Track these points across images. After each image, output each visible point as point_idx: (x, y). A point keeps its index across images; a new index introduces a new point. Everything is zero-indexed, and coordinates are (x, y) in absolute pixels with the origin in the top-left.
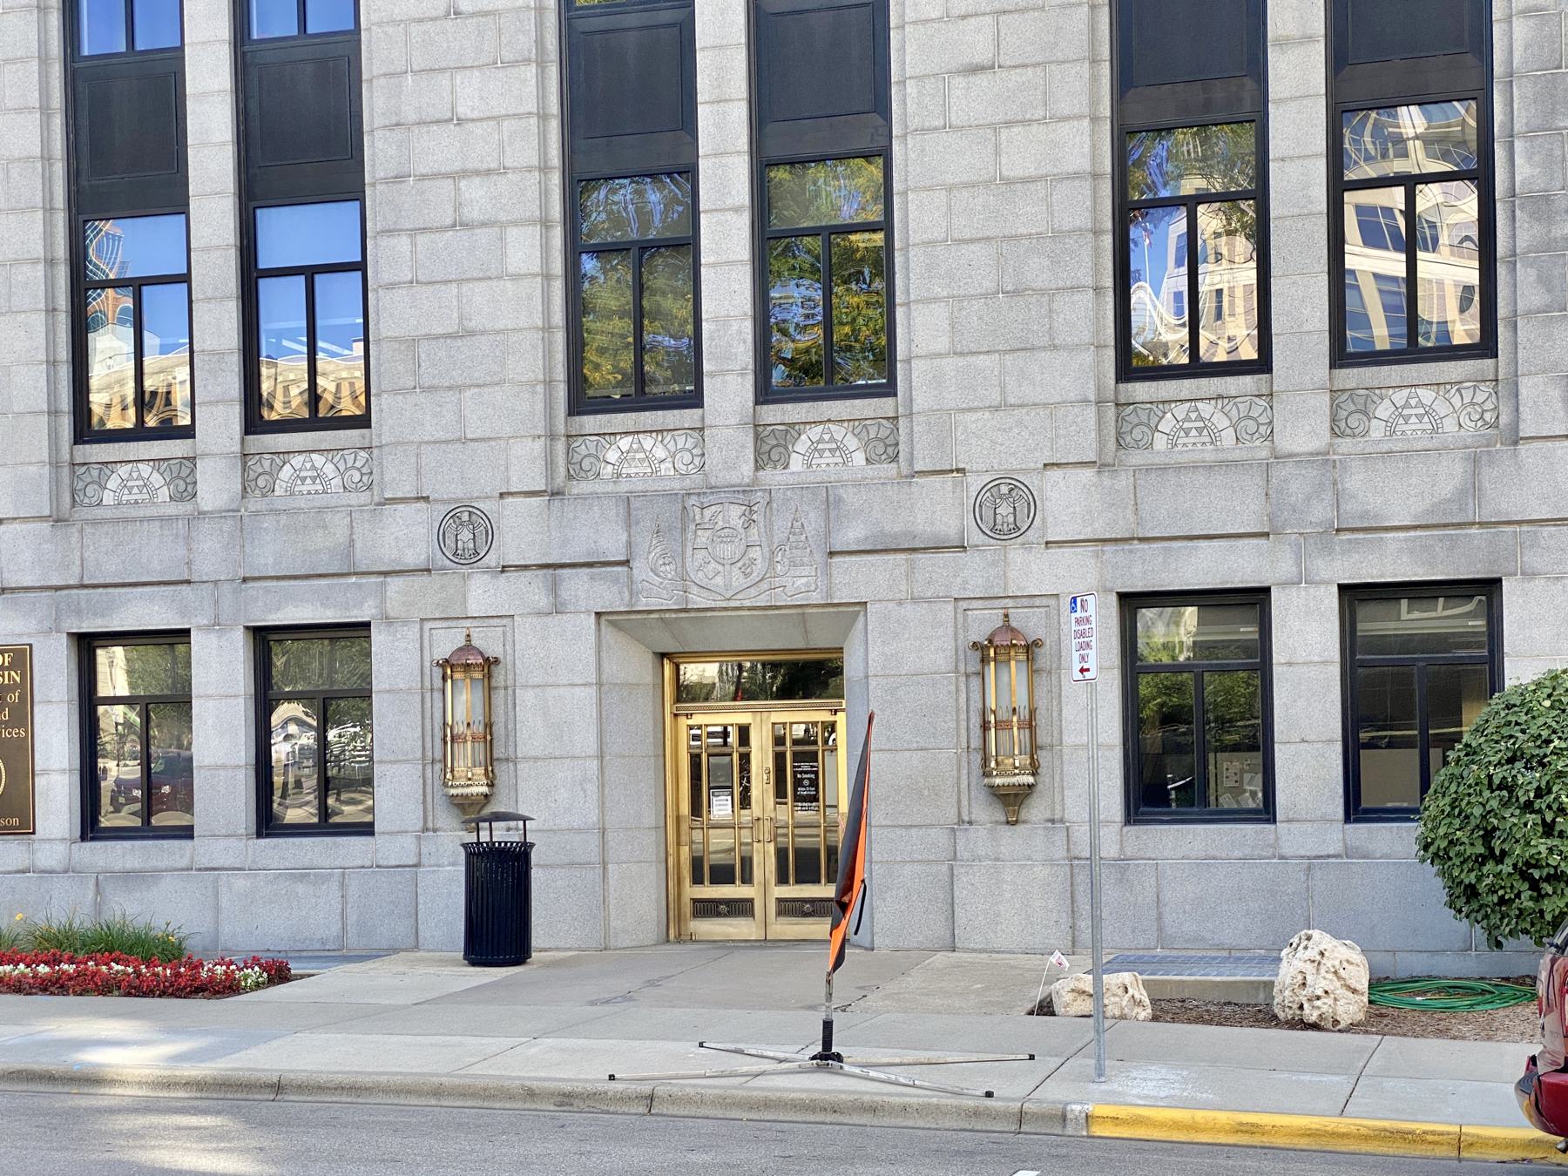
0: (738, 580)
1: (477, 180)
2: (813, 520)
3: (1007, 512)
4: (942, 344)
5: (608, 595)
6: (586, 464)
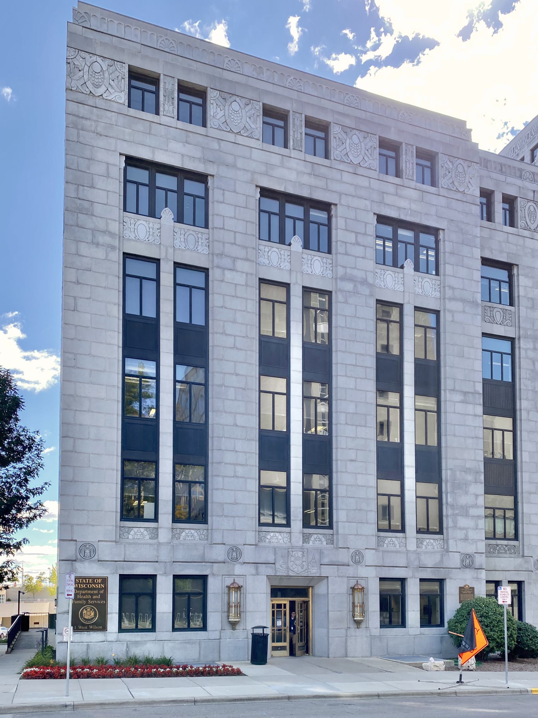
0: (300, 570)
1: (240, 467)
2: (317, 557)
4: (345, 520)
5: (271, 572)
6: (262, 538)
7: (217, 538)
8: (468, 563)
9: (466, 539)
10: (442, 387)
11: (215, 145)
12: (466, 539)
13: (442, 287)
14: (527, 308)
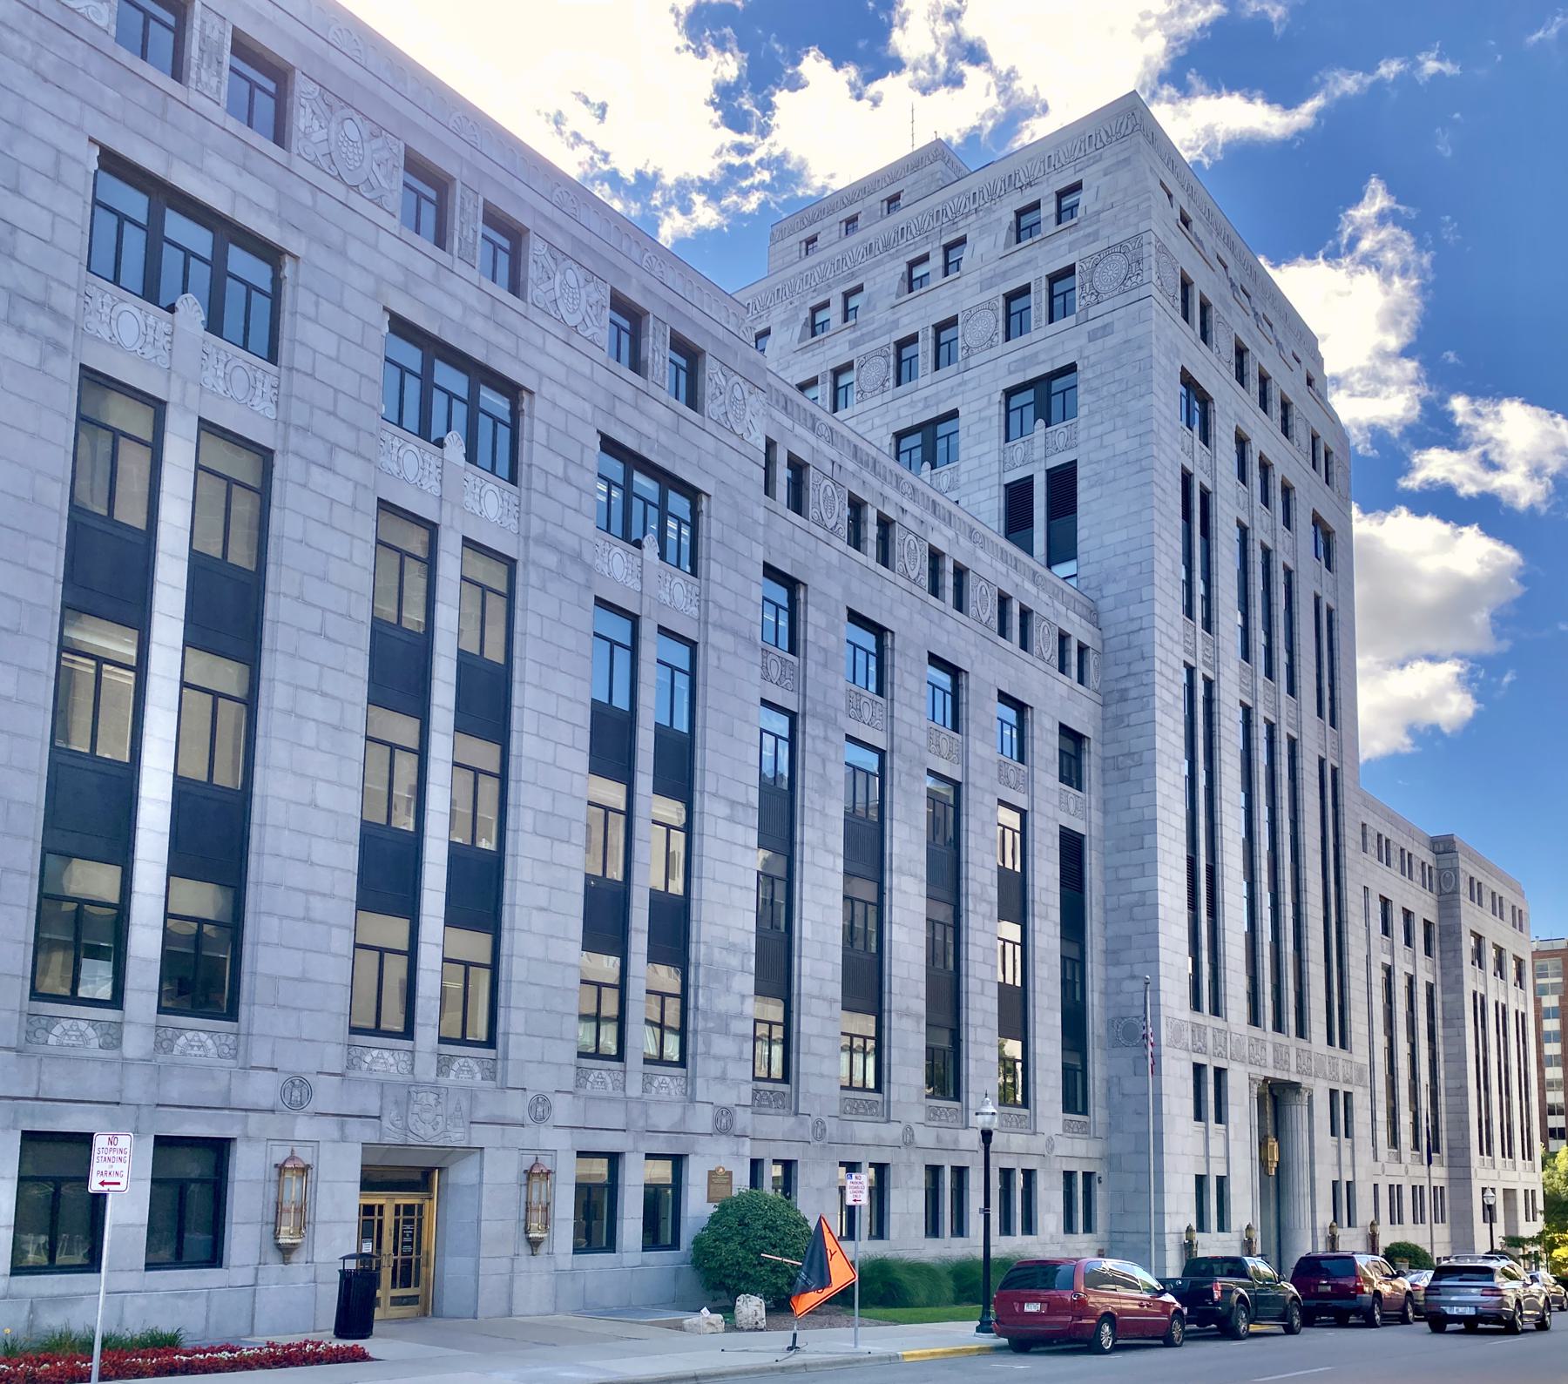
0: (431, 1132)
2: (465, 1105)
3: (540, 1110)
5: (370, 1135)
7: (261, 1055)
8: (724, 1126)
9: (723, 1078)
10: (697, 786)
11: (305, 195)
12: (723, 1078)
13: (704, 601)
14: (817, 663)
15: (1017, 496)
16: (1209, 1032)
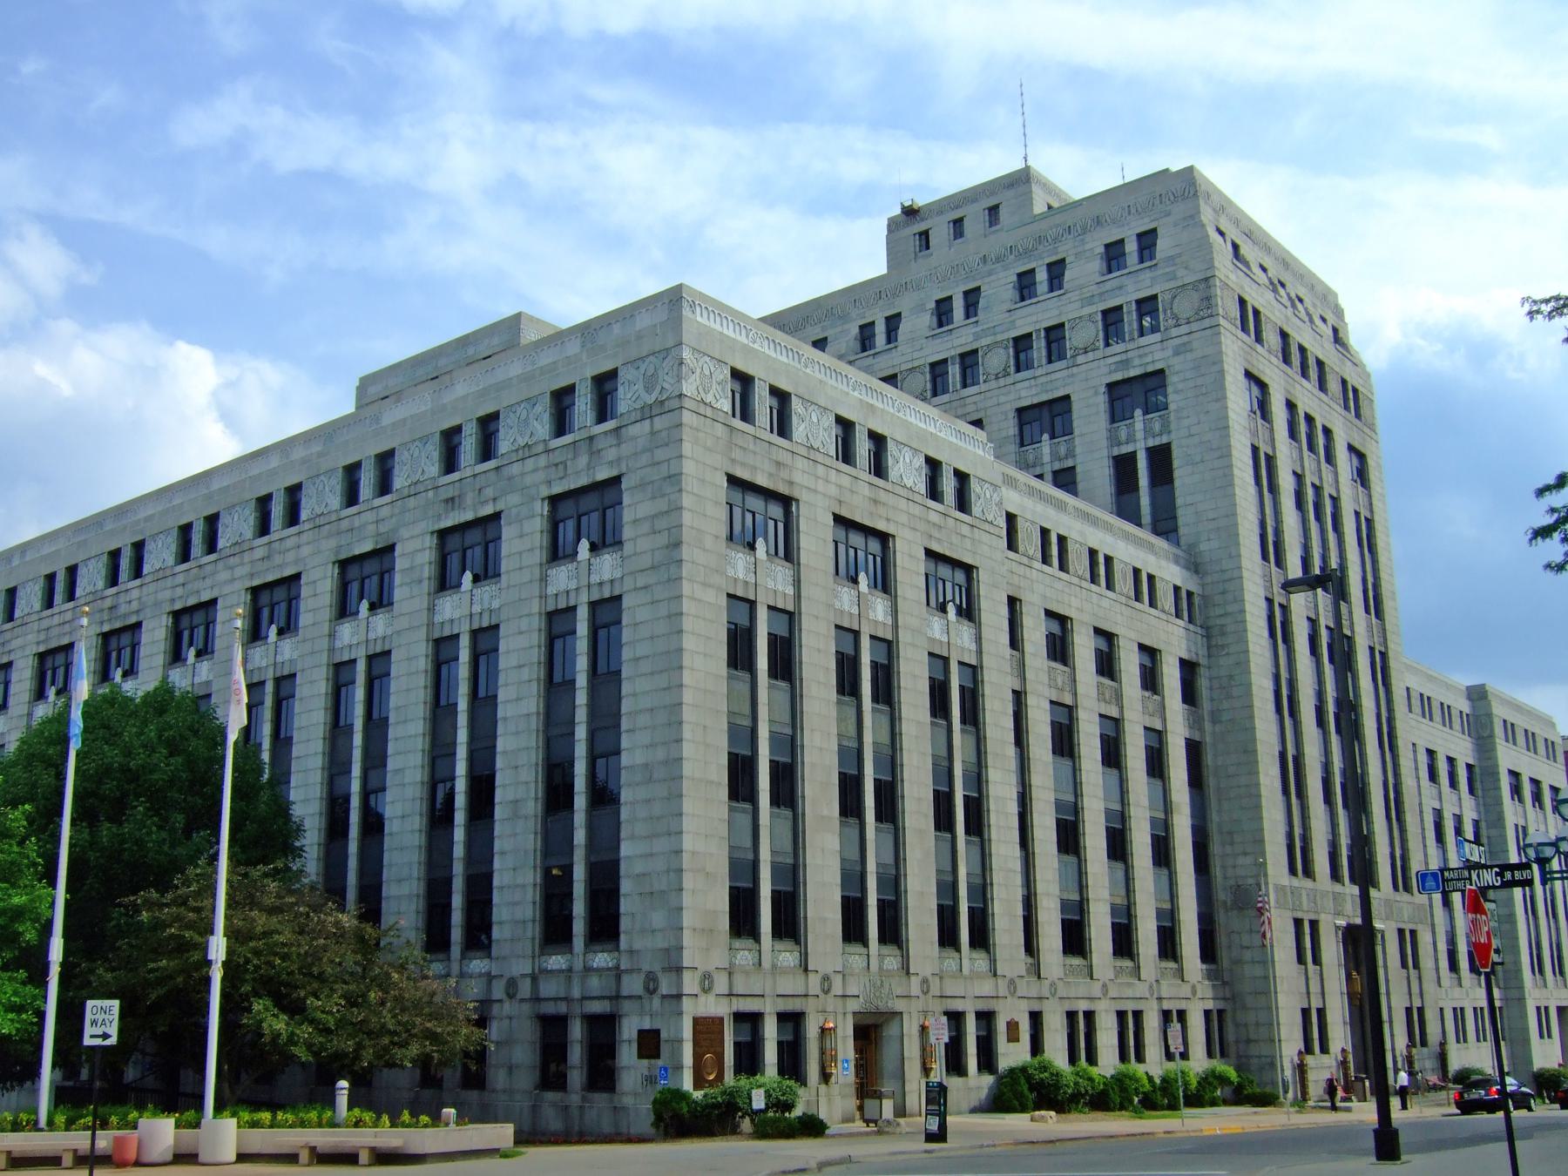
15: (1124, 467)
16: (1304, 893)
